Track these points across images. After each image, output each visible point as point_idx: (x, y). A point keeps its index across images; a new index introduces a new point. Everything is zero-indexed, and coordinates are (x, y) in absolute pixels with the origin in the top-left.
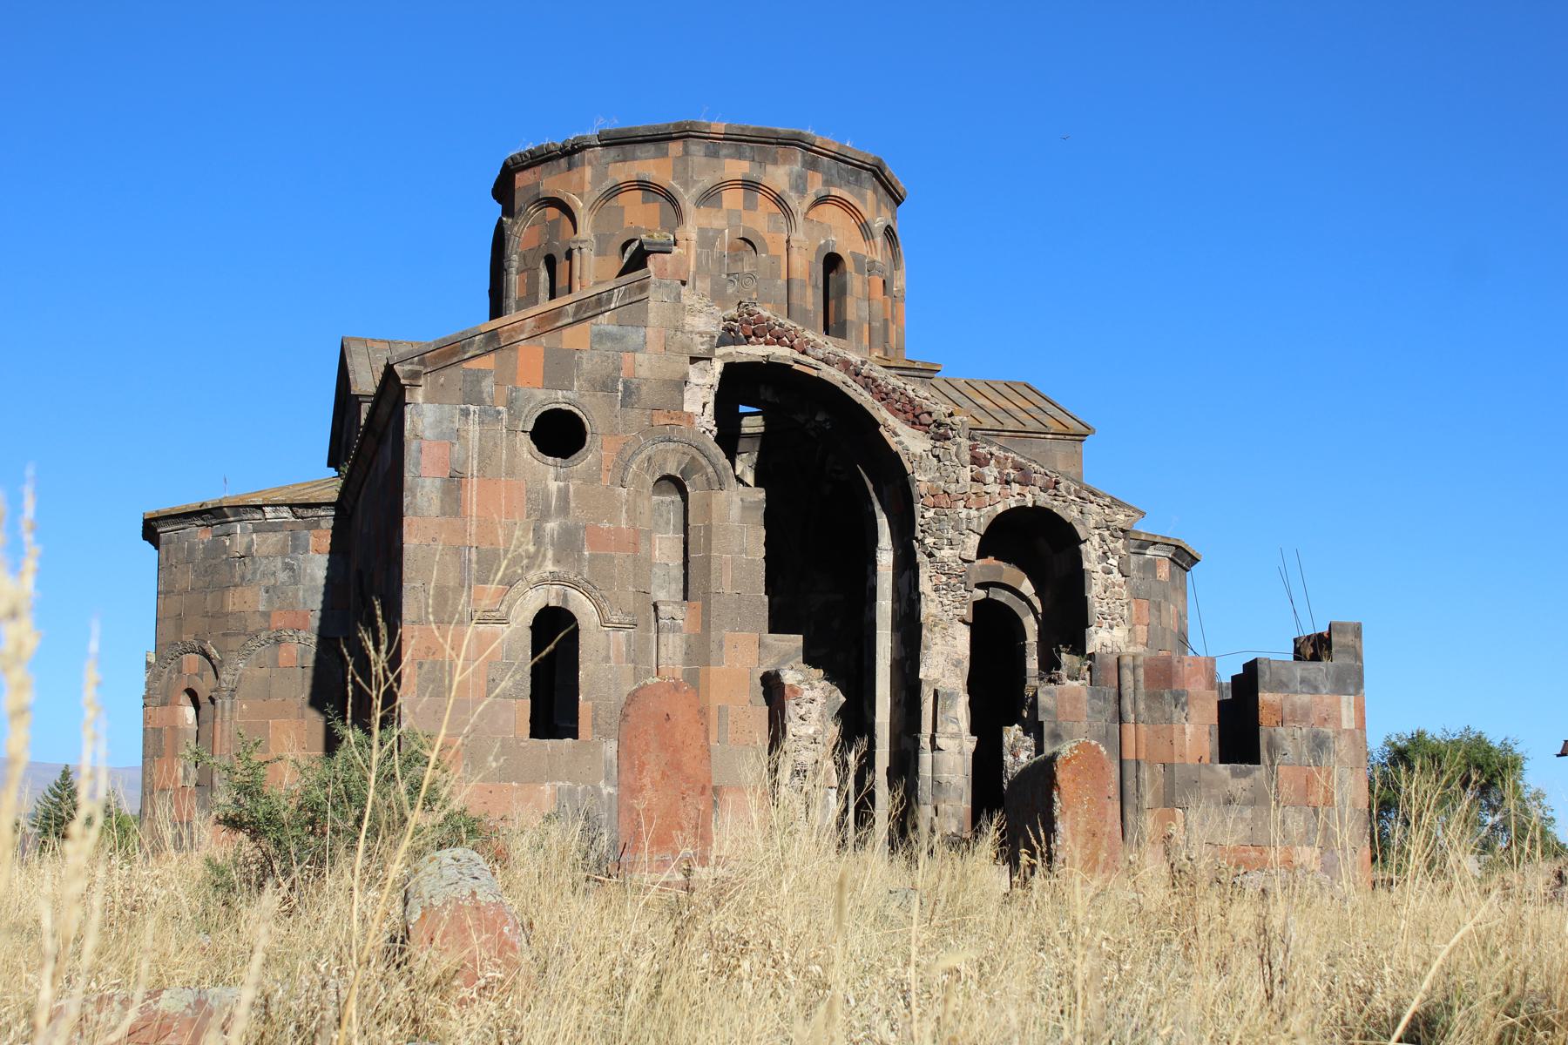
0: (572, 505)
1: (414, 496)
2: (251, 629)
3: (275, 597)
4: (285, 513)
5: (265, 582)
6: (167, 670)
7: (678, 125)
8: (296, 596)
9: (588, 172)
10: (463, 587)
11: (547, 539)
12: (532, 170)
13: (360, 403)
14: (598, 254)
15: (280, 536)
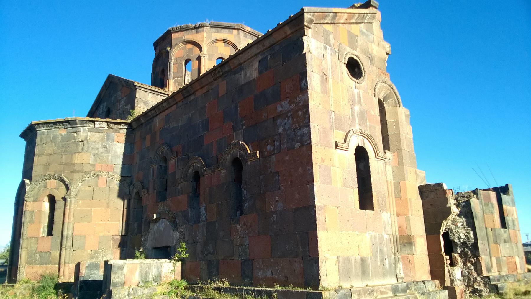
0: (362, 101)
1: (311, 80)
2: (85, 170)
3: (98, 158)
4: (105, 125)
5: (93, 152)
6: (38, 186)
7: (237, 25)
8: (108, 159)
9: (205, 34)
10: (331, 130)
11: (356, 115)
12: (180, 33)
13: (136, 89)
14: (209, 60)
15: (101, 134)
